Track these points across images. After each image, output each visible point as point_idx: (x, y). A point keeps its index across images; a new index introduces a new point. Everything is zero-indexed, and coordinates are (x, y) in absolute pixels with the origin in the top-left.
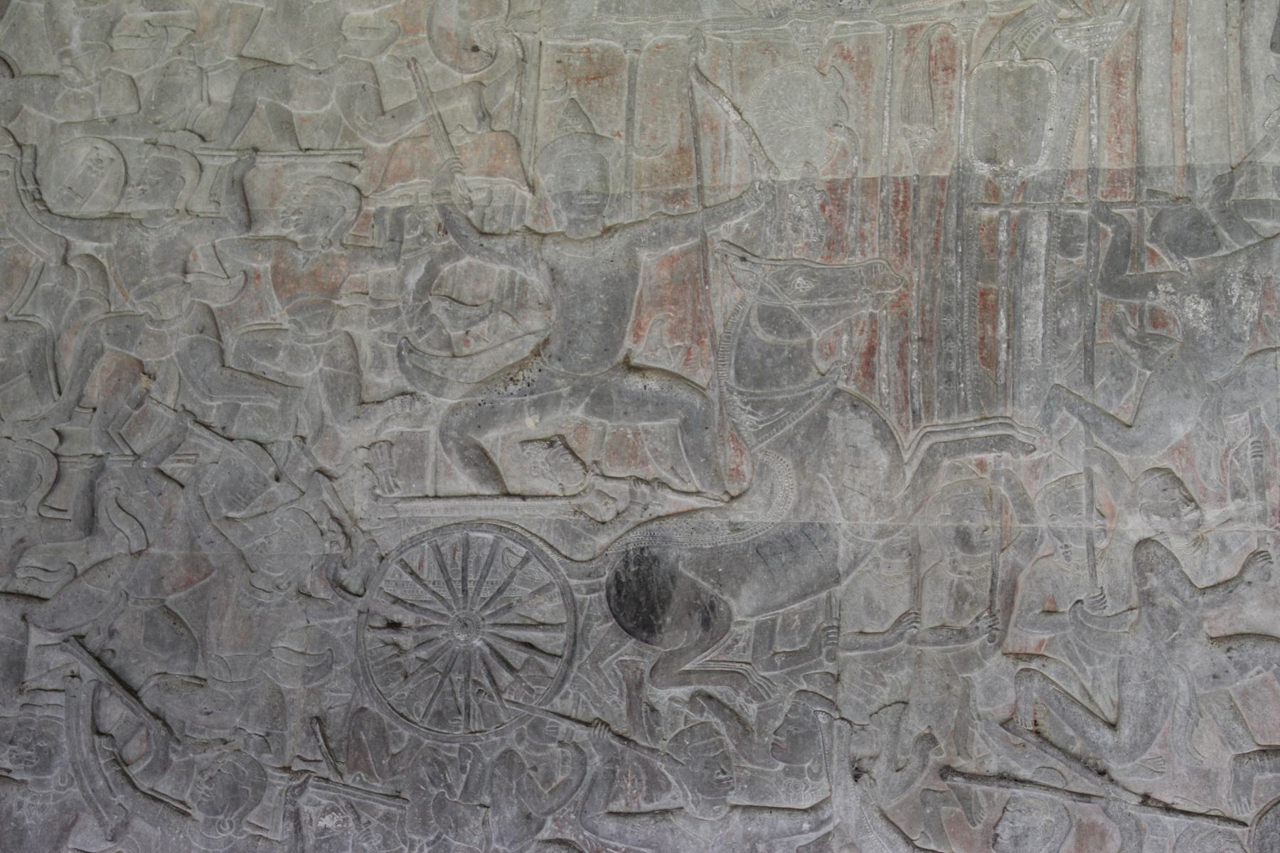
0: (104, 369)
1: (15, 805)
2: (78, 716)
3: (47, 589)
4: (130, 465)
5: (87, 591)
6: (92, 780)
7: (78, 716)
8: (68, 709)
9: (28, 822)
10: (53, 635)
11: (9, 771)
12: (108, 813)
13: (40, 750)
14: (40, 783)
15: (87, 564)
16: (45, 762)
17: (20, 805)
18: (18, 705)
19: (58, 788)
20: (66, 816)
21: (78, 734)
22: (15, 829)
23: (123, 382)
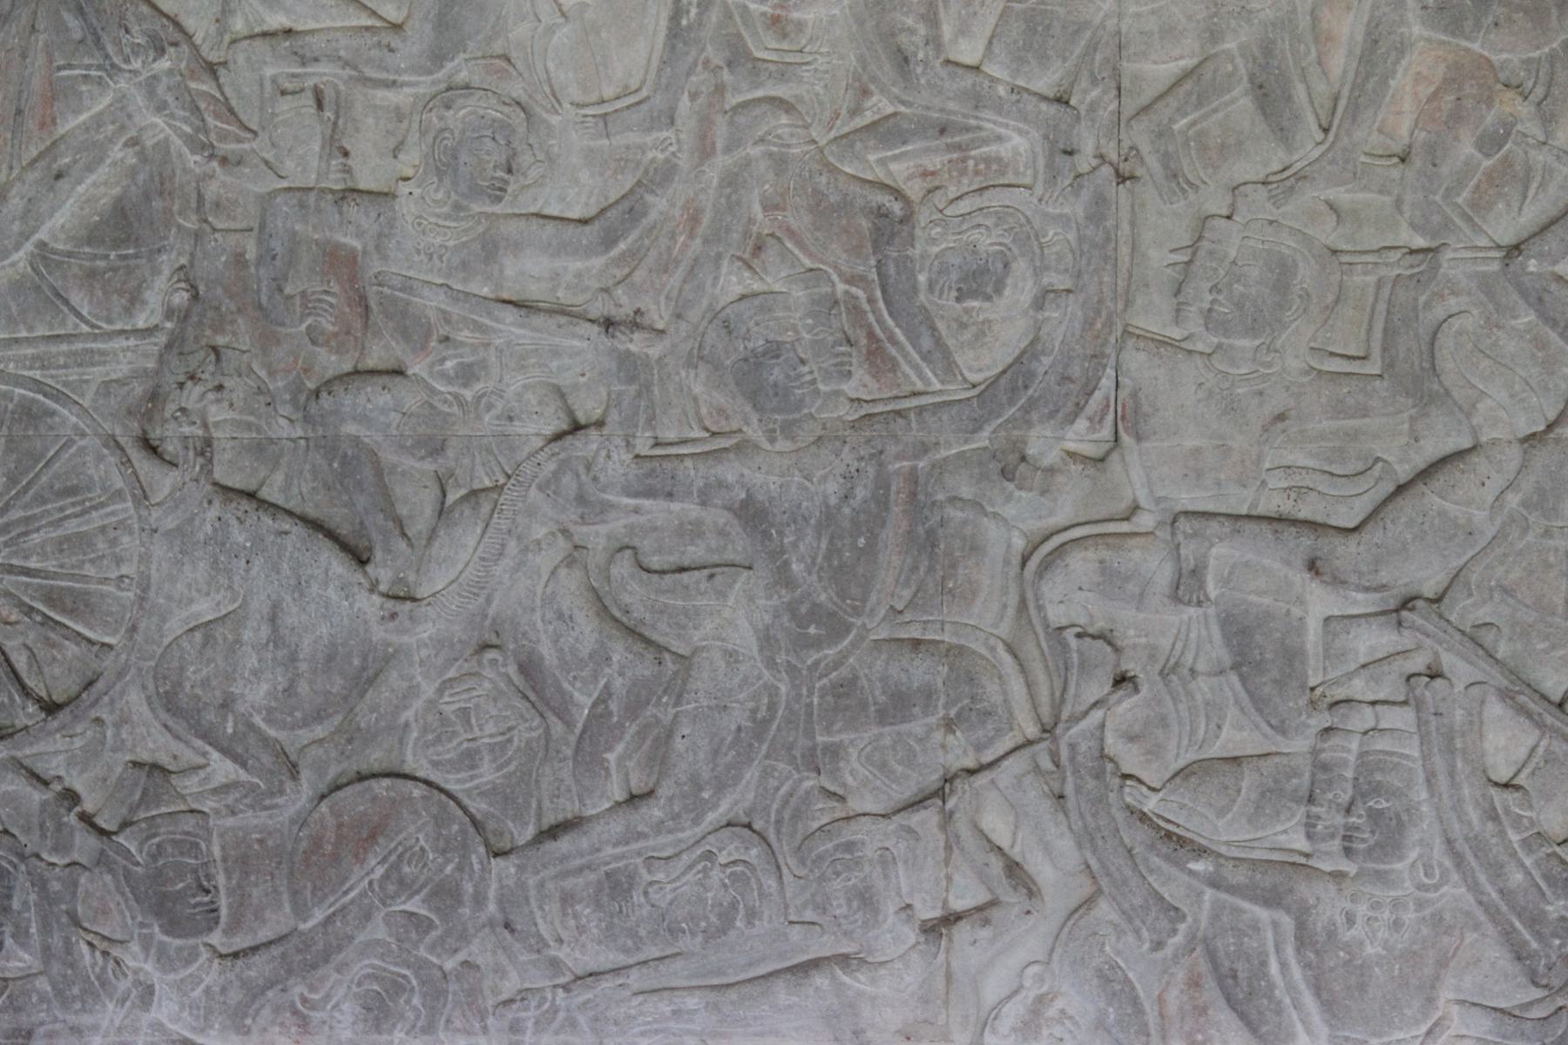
0: (1418, 78)
1: (1340, 920)
2: (1450, 750)
3: (1342, 509)
4: (1495, 267)
5: (1442, 513)
6: (1496, 871)
7: (1450, 750)
8: (1424, 739)
9: (1369, 950)
10: (1360, 596)
11: (1307, 856)
12: (1539, 936)
13: (1375, 816)
14: (1381, 877)
15: (1420, 462)
16: (1389, 834)
17: (1350, 920)
18: (1314, 731)
19: (1421, 887)
20: (1446, 939)
21: (1454, 785)
22: (1347, 963)
23: (1469, 103)
